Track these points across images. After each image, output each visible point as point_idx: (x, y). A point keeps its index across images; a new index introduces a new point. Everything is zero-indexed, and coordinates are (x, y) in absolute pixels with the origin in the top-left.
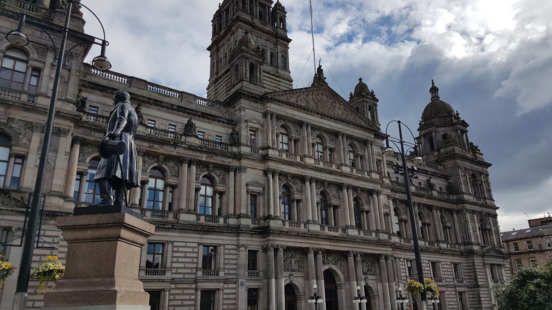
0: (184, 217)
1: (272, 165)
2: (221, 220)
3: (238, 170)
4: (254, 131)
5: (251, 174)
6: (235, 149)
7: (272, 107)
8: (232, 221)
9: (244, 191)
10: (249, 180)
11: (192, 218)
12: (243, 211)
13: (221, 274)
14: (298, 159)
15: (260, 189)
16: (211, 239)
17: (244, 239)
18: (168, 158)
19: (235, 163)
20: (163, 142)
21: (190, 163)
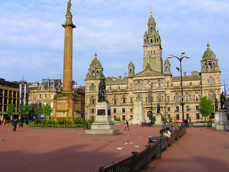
0: (118, 104)
1: (134, 92)
2: (125, 104)
3: (128, 94)
4: (131, 85)
5: (131, 94)
6: (127, 89)
7: (134, 79)
8: (127, 104)
9: (129, 98)
10: (130, 95)
11: (120, 104)
12: (129, 102)
13: (125, 113)
14: (141, 89)
15: (132, 97)
16: (123, 107)
17: (129, 107)
18: (116, 94)
19: (127, 92)
20: (114, 92)
21: (119, 94)
